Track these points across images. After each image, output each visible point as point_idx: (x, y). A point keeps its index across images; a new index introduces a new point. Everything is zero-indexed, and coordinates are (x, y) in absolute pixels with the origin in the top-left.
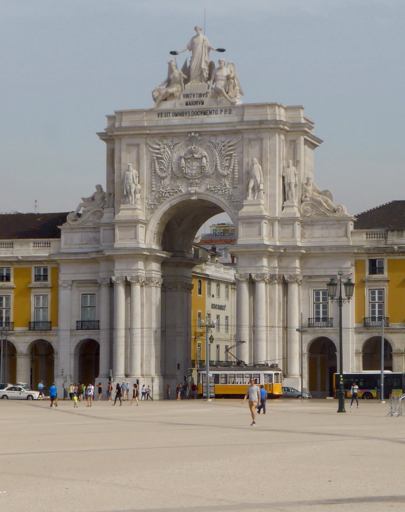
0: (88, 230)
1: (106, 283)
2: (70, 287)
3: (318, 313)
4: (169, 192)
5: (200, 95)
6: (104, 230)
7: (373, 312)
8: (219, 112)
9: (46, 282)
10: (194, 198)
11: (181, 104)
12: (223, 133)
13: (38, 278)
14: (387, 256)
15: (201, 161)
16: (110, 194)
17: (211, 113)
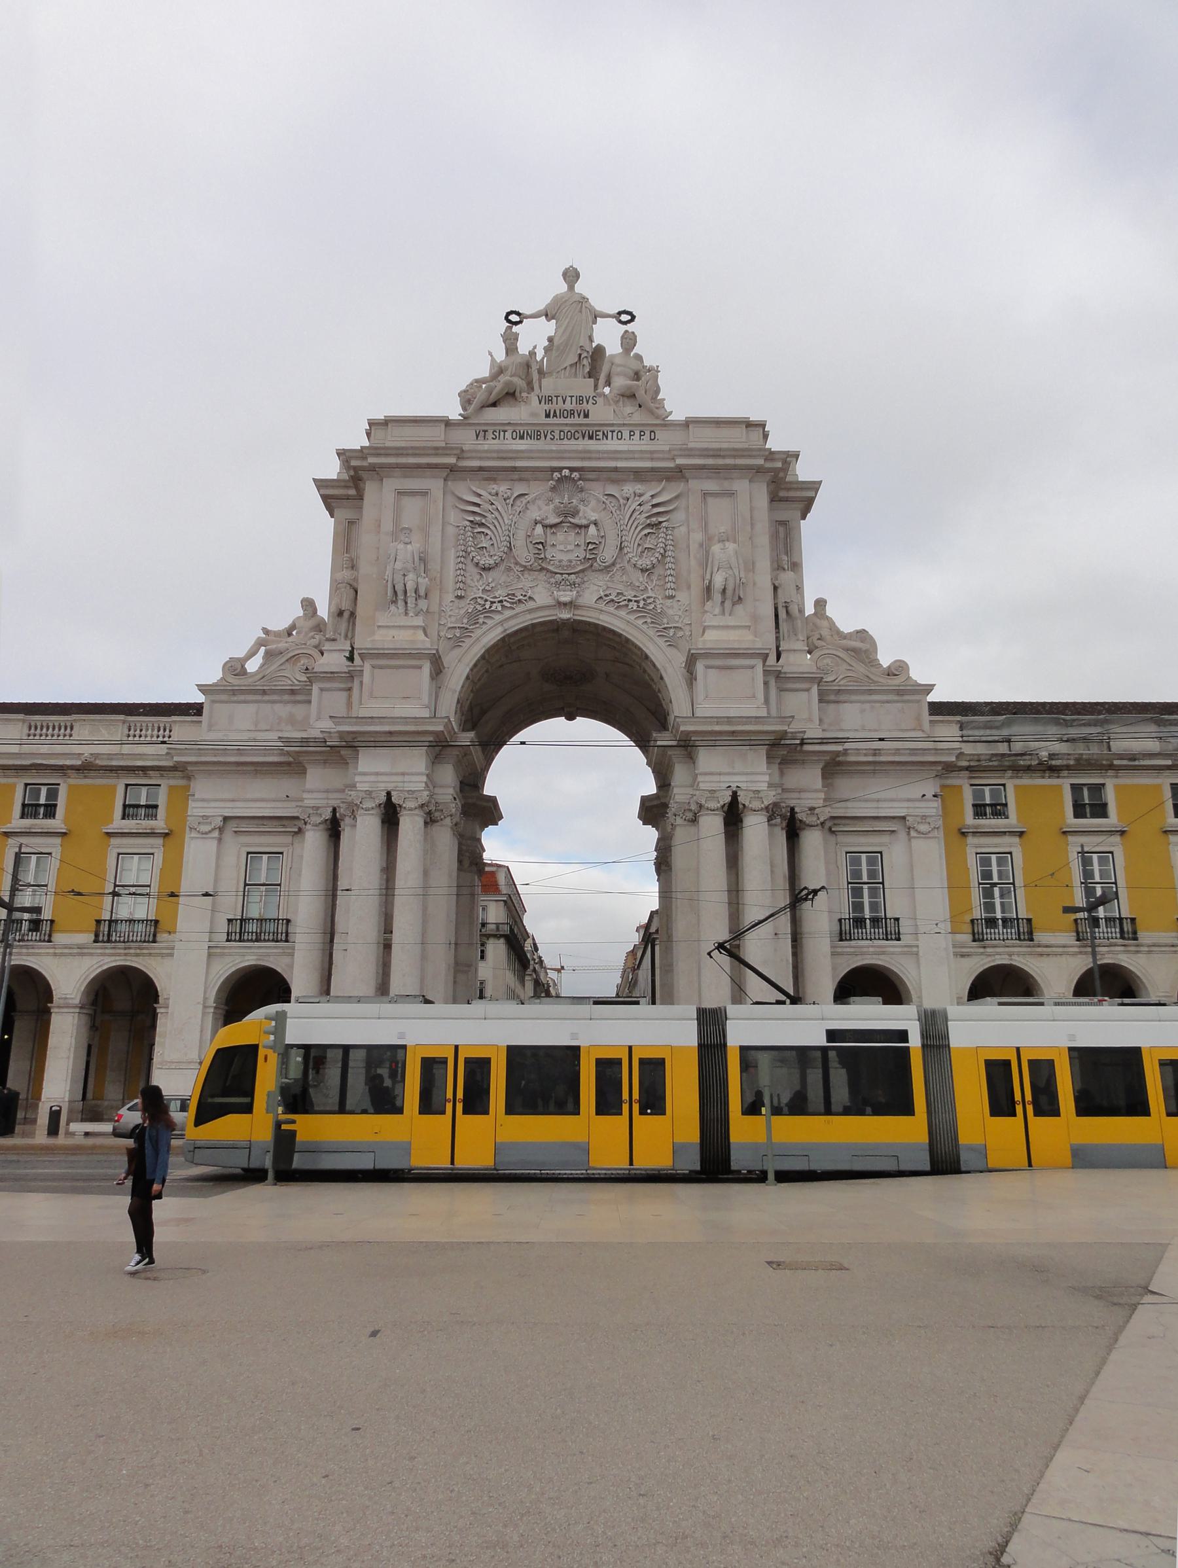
0: (275, 697)
1: (319, 820)
2: (216, 834)
3: (858, 907)
4: (501, 601)
5: (580, 400)
6: (322, 690)
7: (989, 907)
8: (626, 434)
9: (152, 823)
10: (565, 615)
11: (534, 415)
12: (639, 475)
13: (129, 811)
14: (1012, 778)
15: (586, 534)
16: (340, 613)
17: (605, 436)
